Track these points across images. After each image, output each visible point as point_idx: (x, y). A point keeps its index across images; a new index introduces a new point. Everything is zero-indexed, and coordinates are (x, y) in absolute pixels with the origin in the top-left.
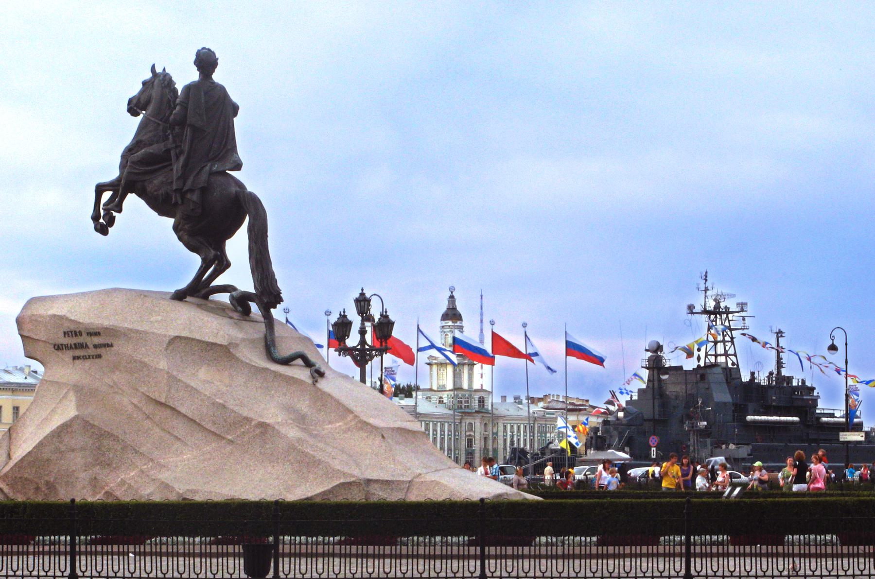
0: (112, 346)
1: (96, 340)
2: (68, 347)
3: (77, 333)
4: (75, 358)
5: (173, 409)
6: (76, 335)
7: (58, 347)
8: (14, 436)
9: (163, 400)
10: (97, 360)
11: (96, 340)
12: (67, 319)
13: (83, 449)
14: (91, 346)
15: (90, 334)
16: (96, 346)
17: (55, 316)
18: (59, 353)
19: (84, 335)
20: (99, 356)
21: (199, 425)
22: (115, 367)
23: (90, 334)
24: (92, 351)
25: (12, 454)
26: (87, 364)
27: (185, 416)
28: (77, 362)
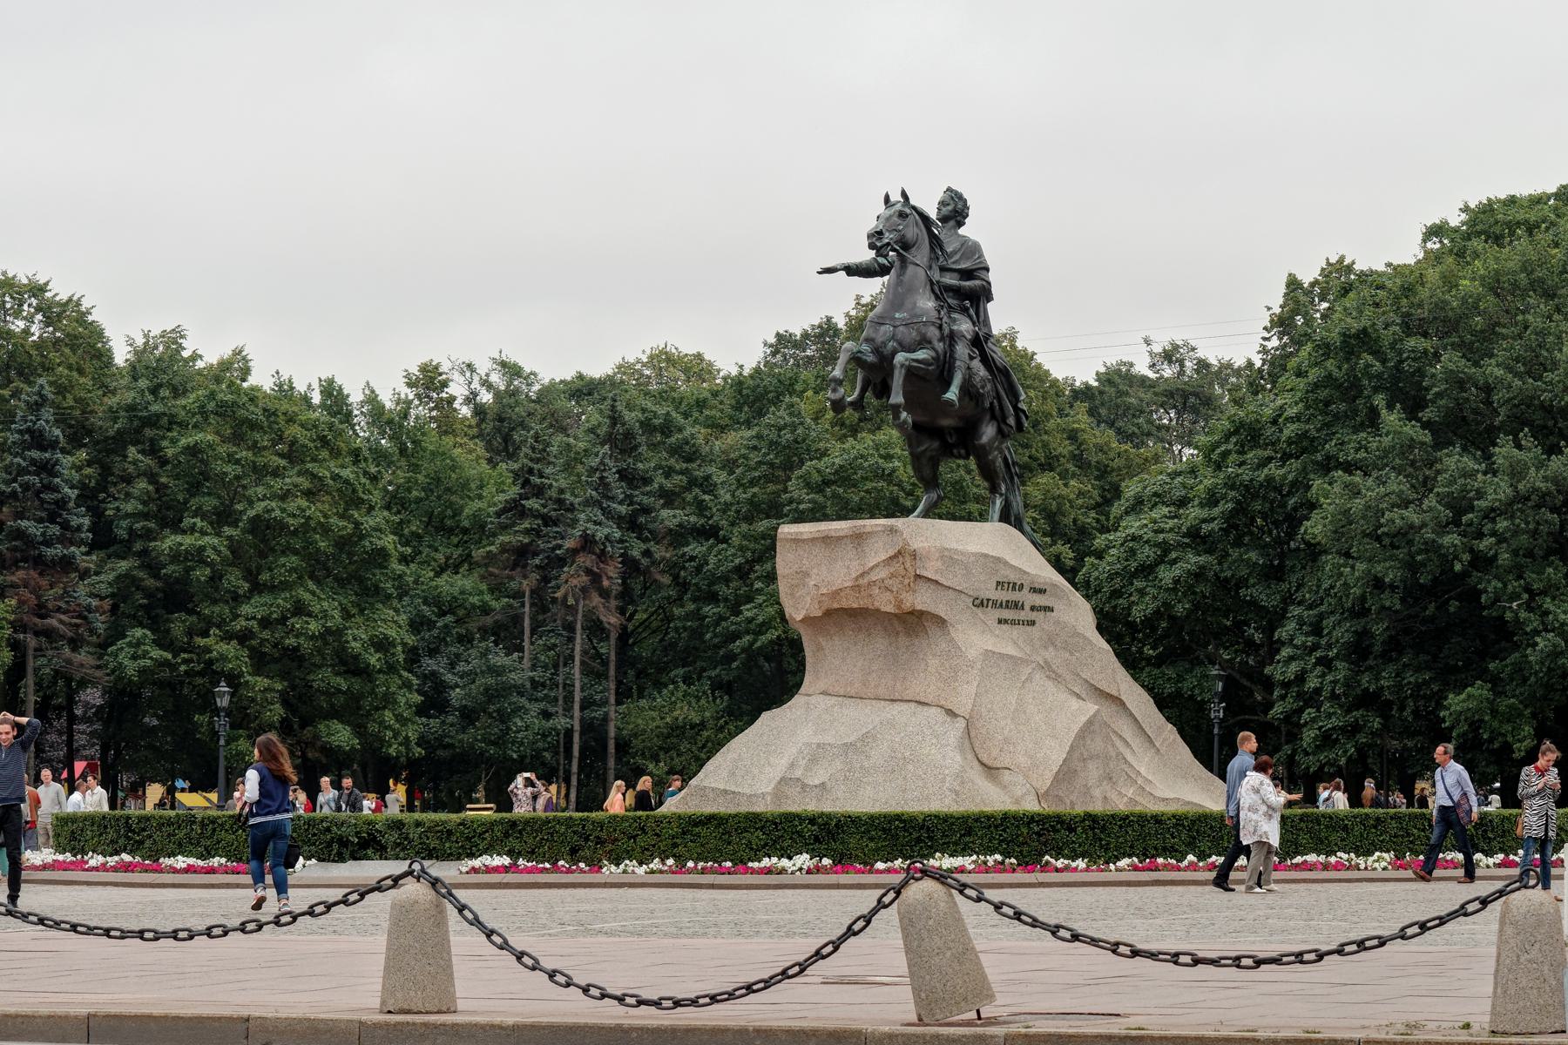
0: (1052, 610)
1: (1039, 600)
2: (997, 605)
3: (1015, 587)
4: (1000, 622)
5: (1123, 704)
6: (1014, 589)
7: (981, 603)
8: (973, 734)
9: (1114, 693)
10: (1029, 628)
11: (1039, 600)
12: (1006, 563)
13: (1098, 756)
14: (1027, 607)
15: (1034, 590)
16: (1033, 608)
17: (986, 556)
18: (979, 611)
19: (1026, 590)
20: (1033, 623)
21: (1141, 727)
22: (1050, 641)
23: (1034, 590)
24: (1025, 615)
25: (985, 760)
26: (1016, 631)
27: (1131, 714)
28: (1005, 627)
